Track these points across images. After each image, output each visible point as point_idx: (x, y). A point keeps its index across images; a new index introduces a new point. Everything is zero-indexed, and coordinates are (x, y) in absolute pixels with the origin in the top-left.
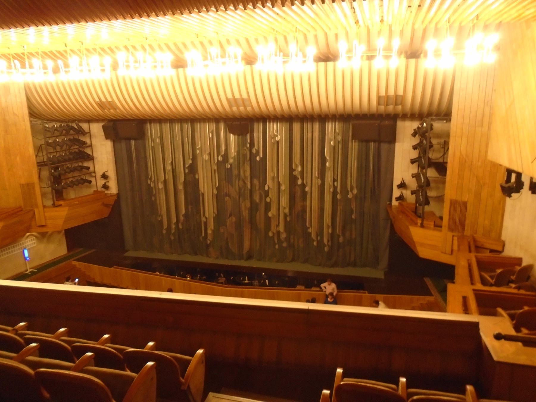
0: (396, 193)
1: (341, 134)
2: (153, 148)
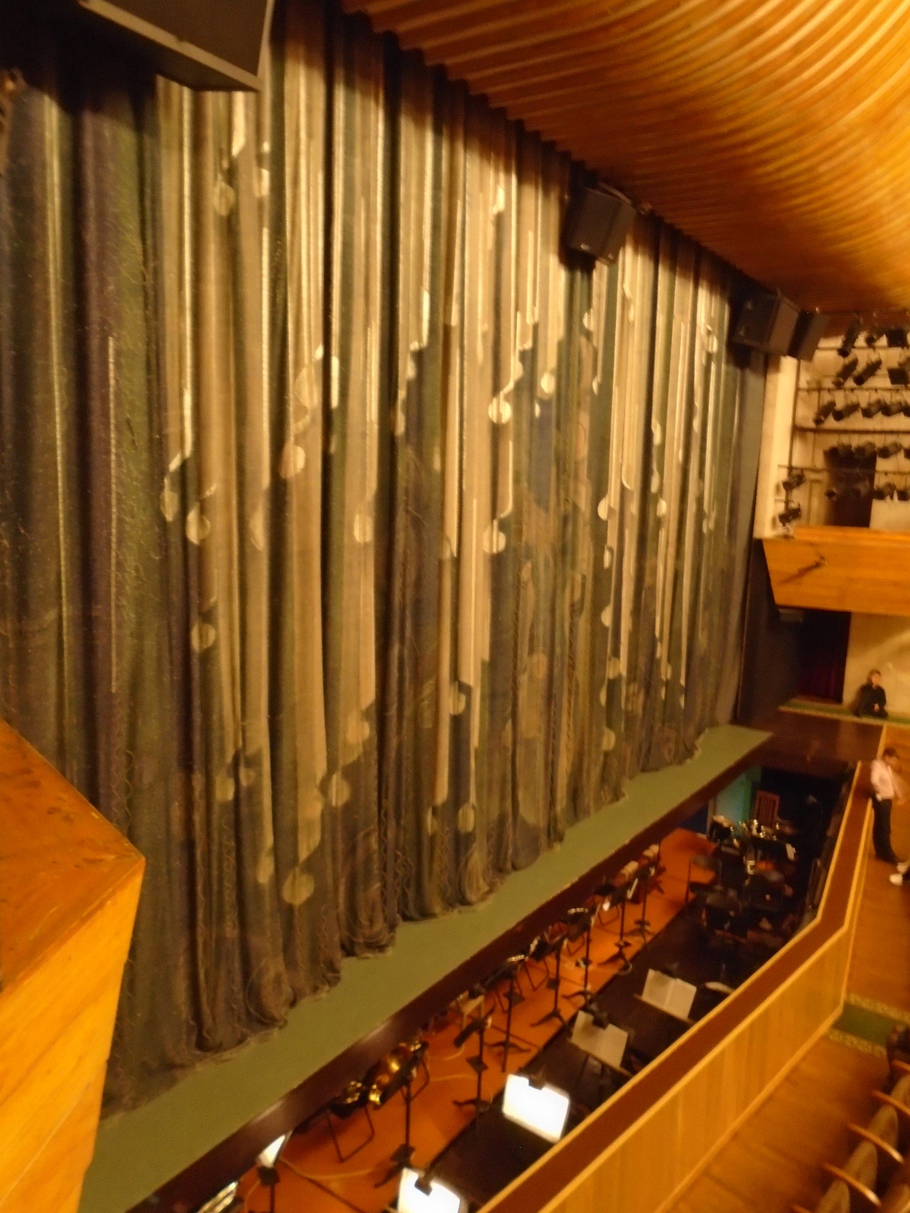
0: (770, 506)
1: (716, 331)
2: (230, 226)
